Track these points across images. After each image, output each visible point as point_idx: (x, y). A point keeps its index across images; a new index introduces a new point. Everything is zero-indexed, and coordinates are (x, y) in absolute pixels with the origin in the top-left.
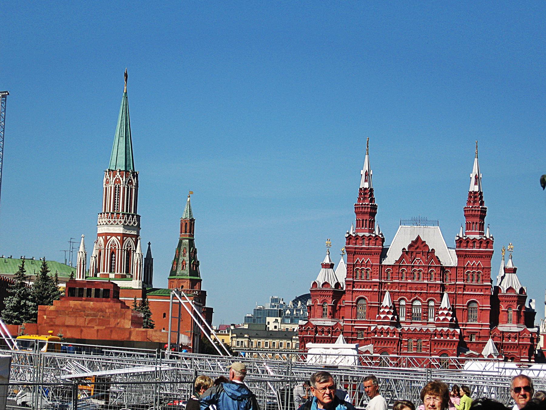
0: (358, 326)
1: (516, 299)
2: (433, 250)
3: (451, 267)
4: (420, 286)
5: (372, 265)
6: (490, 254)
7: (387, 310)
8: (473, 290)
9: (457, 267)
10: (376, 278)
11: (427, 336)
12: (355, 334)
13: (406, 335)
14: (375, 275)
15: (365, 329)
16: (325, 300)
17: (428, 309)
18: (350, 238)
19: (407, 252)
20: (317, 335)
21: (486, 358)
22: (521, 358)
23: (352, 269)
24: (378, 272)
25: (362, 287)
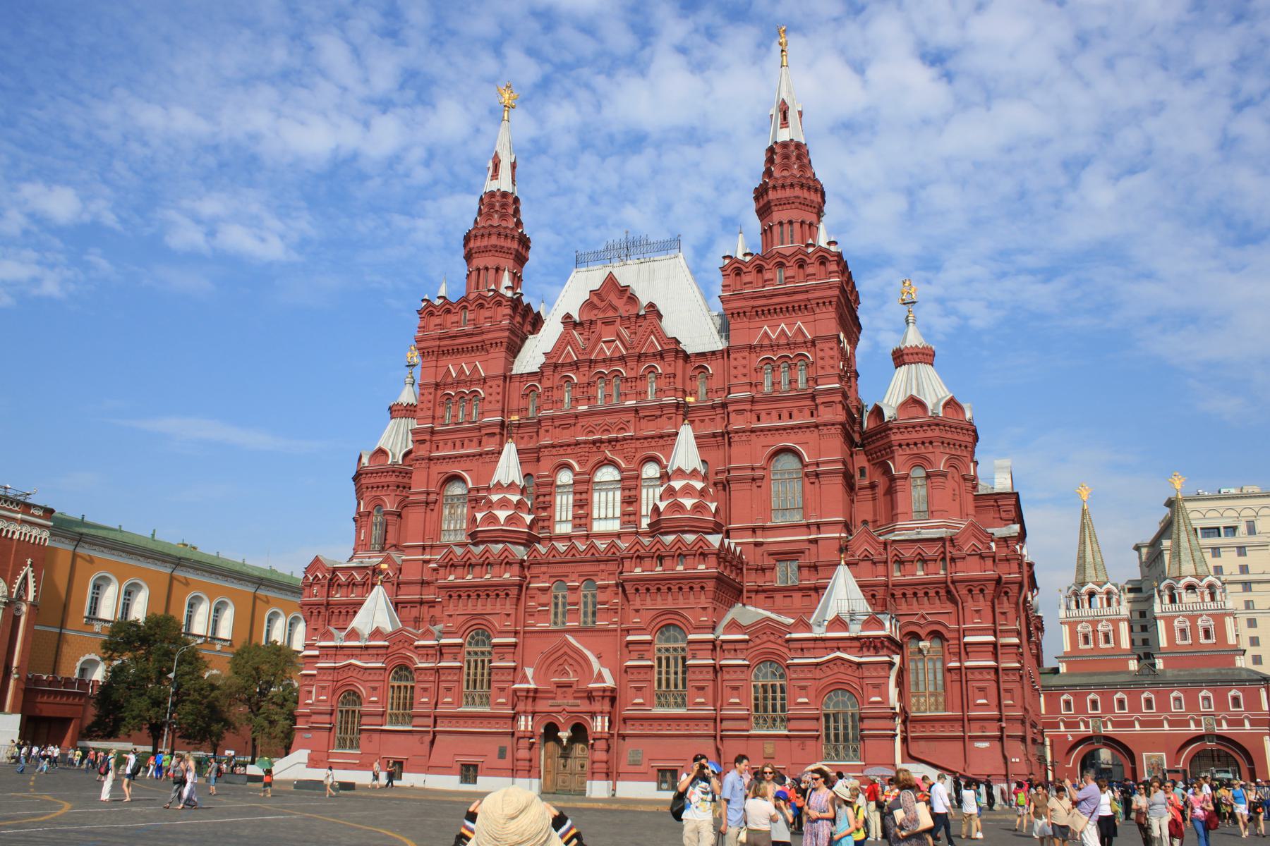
2: (651, 305)
3: (713, 353)
5: (485, 379)
8: (785, 414)
9: (727, 353)
10: (491, 412)
11: (612, 567)
13: (544, 568)
16: (377, 497)
19: (576, 325)
20: (337, 597)
21: (818, 632)
22: (965, 632)
23: (431, 397)
24: (500, 397)
25: (458, 444)
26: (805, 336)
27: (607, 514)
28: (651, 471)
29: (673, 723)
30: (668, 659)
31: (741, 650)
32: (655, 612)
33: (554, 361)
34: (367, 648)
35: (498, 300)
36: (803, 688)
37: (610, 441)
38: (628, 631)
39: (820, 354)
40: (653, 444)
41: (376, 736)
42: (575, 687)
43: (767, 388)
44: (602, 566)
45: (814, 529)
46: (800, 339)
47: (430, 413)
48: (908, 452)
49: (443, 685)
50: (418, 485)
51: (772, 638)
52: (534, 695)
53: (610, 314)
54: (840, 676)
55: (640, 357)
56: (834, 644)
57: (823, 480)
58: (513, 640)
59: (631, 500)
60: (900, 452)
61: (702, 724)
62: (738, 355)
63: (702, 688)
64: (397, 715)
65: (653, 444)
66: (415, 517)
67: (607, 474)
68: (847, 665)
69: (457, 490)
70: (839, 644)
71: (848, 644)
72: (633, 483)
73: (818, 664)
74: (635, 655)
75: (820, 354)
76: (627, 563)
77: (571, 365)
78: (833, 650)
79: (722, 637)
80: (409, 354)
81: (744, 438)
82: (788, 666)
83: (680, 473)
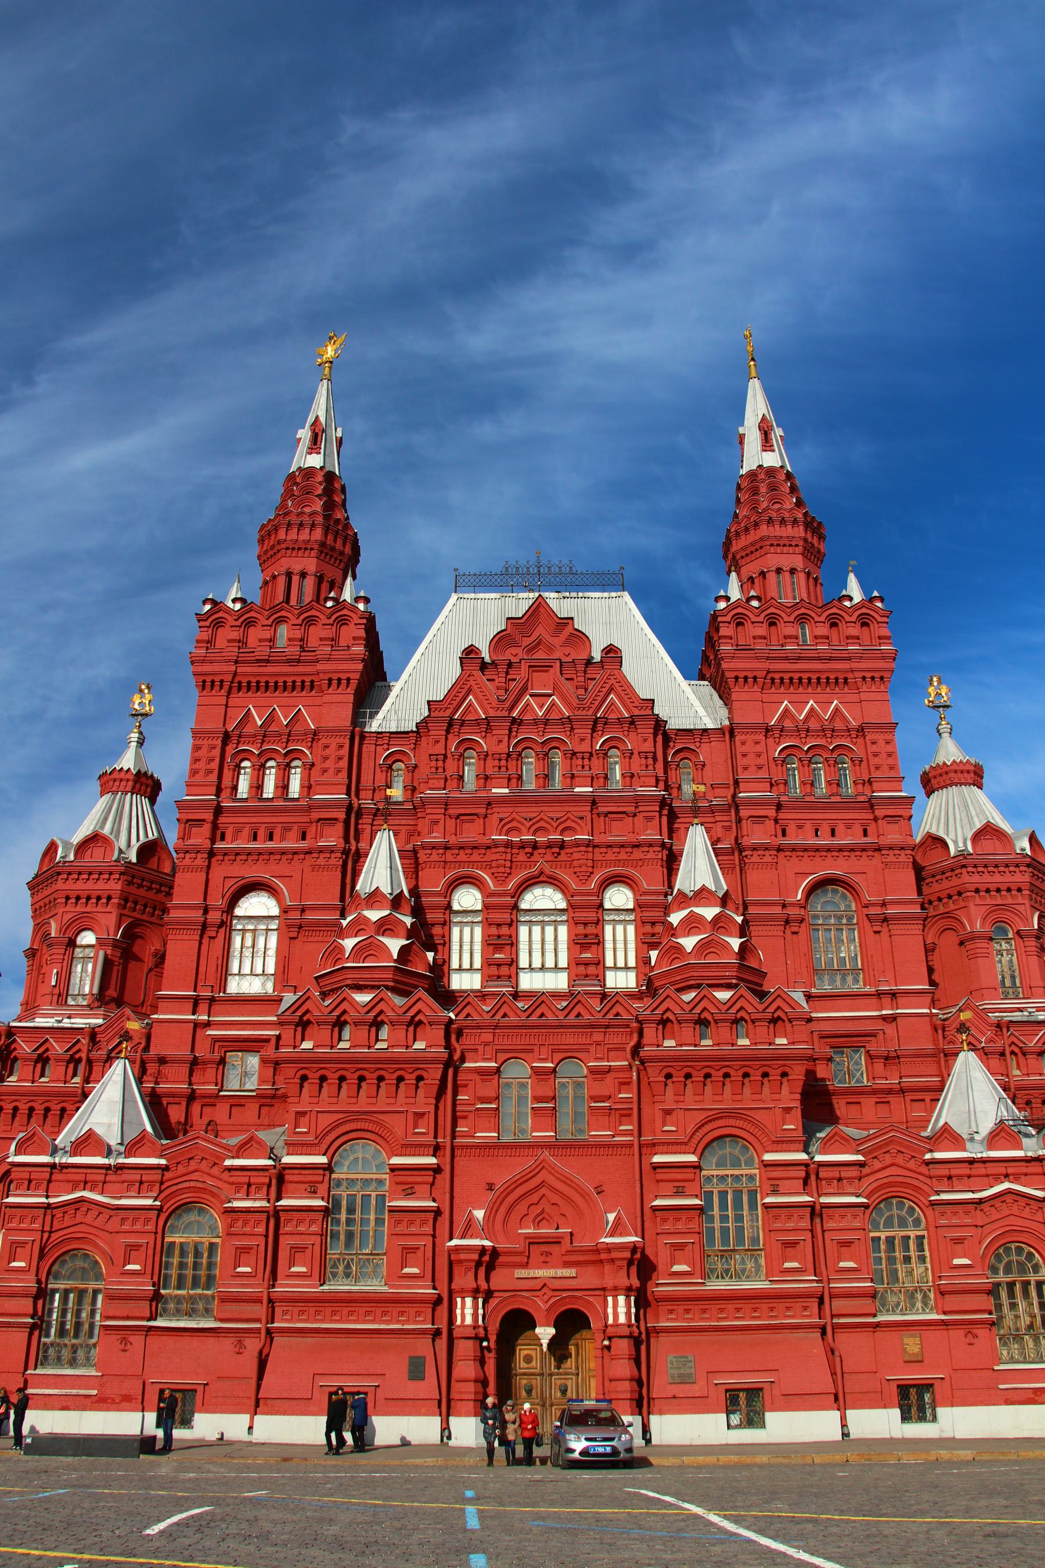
0: (228, 1024)
1: (1023, 877)
2: (612, 653)
4: (556, 811)
5: (315, 733)
6: (880, 664)
7: (374, 915)
10: (328, 788)
11: (615, 1038)
12: (211, 1072)
13: (487, 1037)
14: (324, 778)
15: (266, 1040)
17: (599, 923)
18: (218, 624)
19: (484, 666)
21: (975, 1151)
23: (217, 752)
24: (344, 764)
25: (262, 834)
26: (848, 722)
27: (544, 963)
28: (619, 897)
29: (747, 1307)
30: (723, 1194)
31: (850, 1179)
32: (703, 1115)
33: (448, 713)
34: (120, 1168)
35: (341, 614)
36: (959, 1241)
37: (549, 845)
38: (654, 1147)
39: (874, 748)
40: (623, 856)
41: (137, 1340)
42: (566, 1244)
43: (796, 790)
44: (598, 1036)
45: (887, 1000)
46: (838, 725)
47: (213, 778)
48: (988, 901)
49: (285, 1242)
50: (187, 892)
51: (899, 1160)
52: (489, 1260)
53: (540, 655)
54: (1013, 1220)
55: (596, 725)
56: (1001, 1169)
57: (897, 929)
58: (433, 1160)
59: (587, 942)
60: (978, 901)
61: (798, 1305)
62: (750, 738)
63: (794, 1244)
64: (192, 1299)
65: (623, 856)
66: (180, 950)
67: (543, 898)
68: (1022, 1202)
69: (257, 905)
70: (1007, 1169)
71: (1022, 1168)
72: (591, 916)
73: (980, 1201)
74: (669, 1188)
75: (874, 748)
76: (649, 1032)
77: (478, 722)
78: (998, 1179)
79: (818, 1158)
80: (137, 699)
81: (767, 859)
82: (933, 1204)
83: (702, 895)
